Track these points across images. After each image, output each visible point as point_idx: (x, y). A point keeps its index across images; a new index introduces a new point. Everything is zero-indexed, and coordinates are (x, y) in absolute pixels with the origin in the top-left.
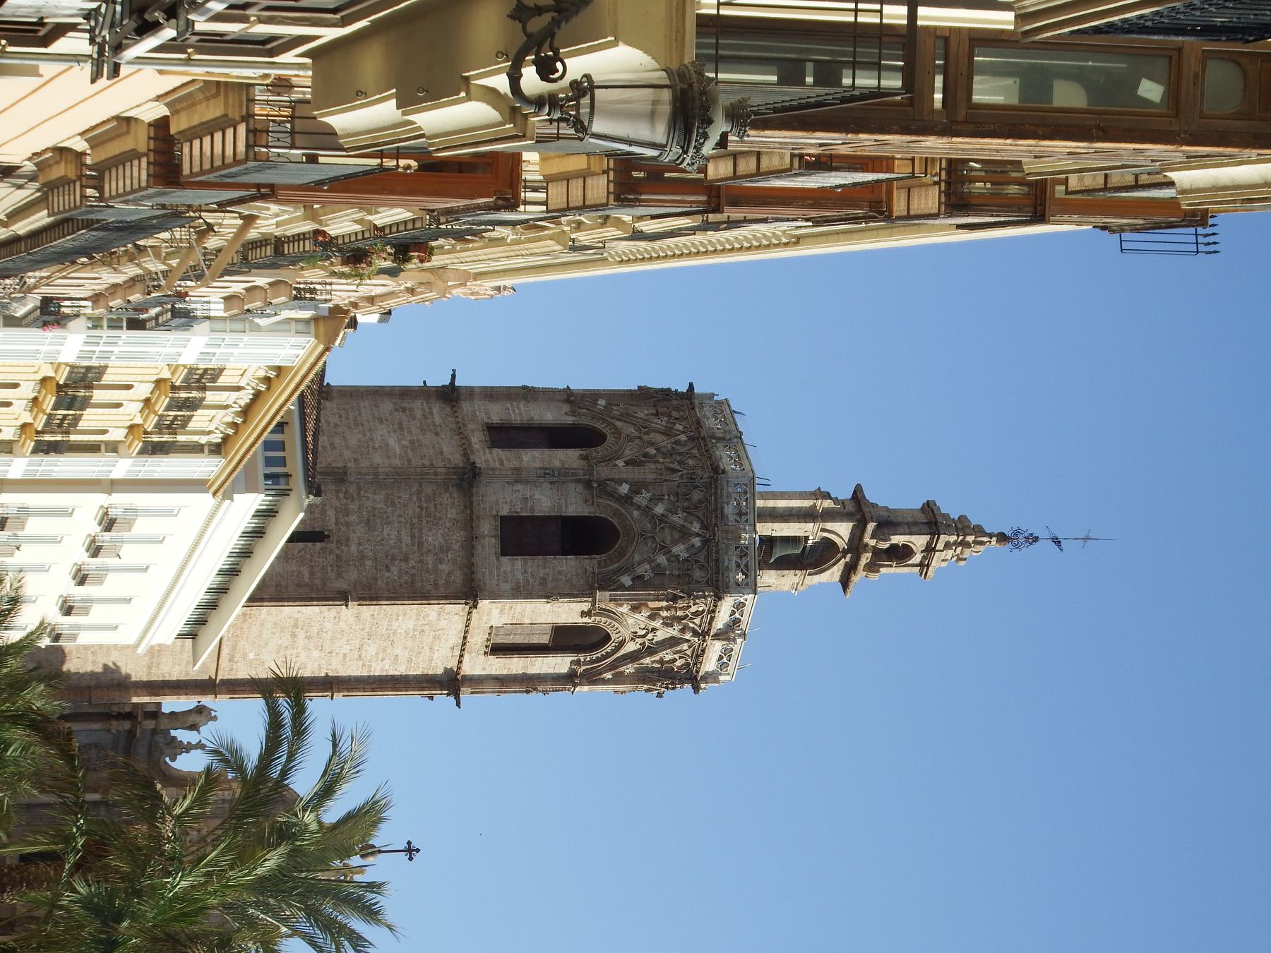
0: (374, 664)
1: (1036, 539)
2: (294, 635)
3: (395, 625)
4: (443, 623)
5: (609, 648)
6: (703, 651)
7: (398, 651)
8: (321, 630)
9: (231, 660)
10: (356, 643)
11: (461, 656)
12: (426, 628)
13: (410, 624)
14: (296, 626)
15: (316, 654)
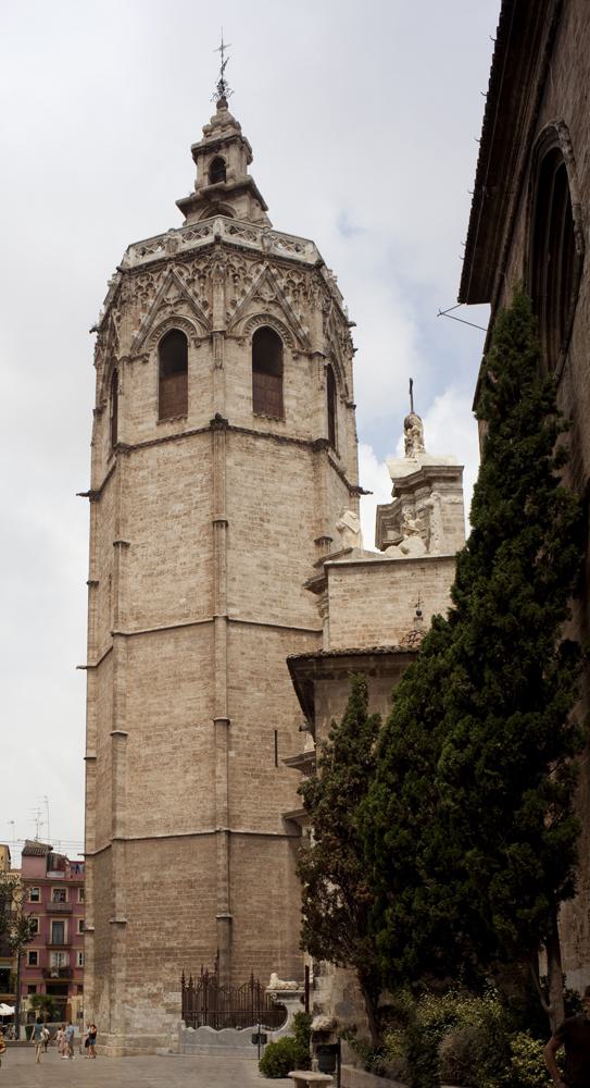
0: (194, 501)
1: (222, 82)
2: (162, 573)
3: (151, 498)
4: (152, 463)
5: (182, 328)
6: (182, 254)
7: (181, 486)
8: (157, 554)
9: (187, 616)
10: (169, 523)
11: (184, 436)
12: (156, 474)
13: (152, 488)
14: (150, 575)
15: (181, 551)
